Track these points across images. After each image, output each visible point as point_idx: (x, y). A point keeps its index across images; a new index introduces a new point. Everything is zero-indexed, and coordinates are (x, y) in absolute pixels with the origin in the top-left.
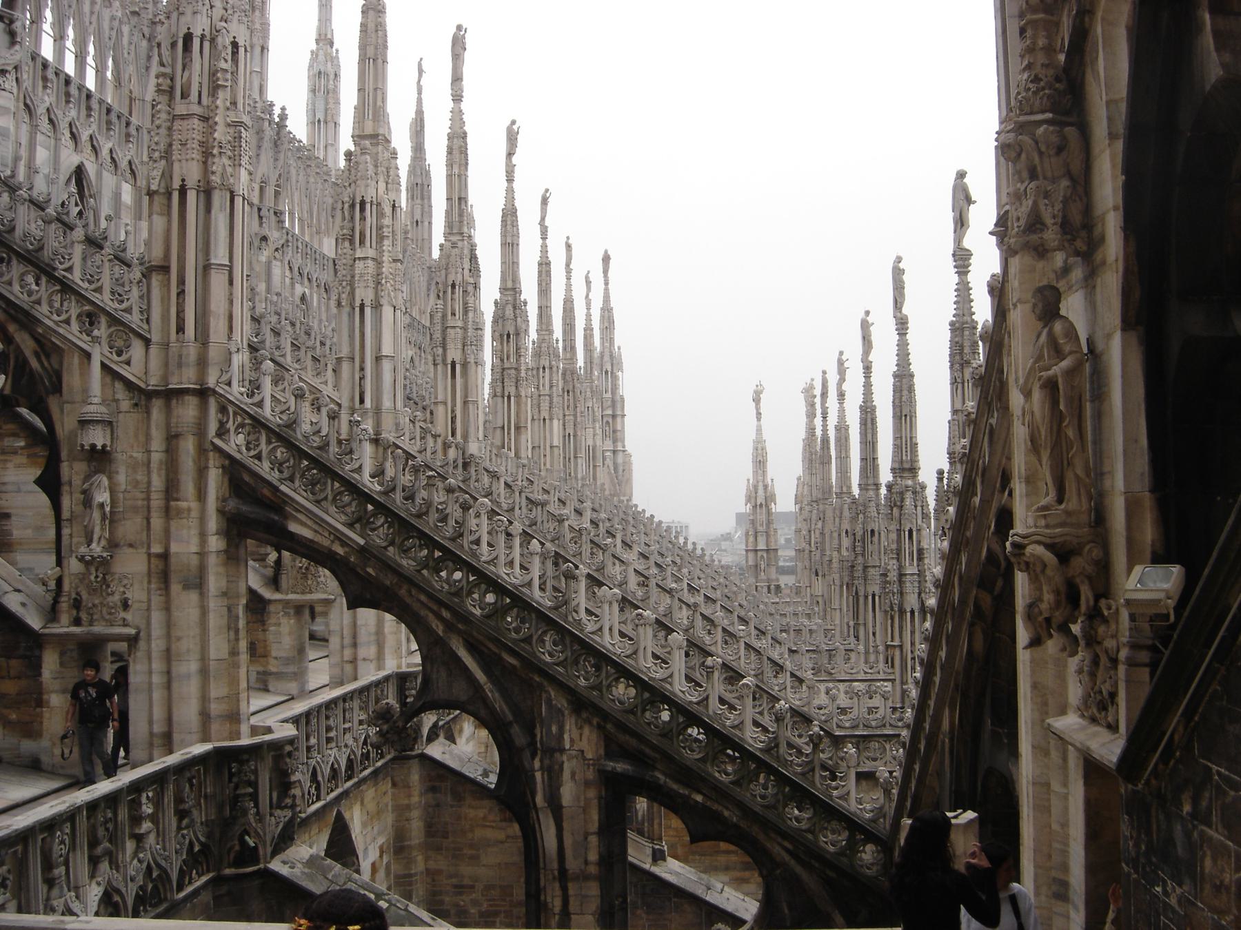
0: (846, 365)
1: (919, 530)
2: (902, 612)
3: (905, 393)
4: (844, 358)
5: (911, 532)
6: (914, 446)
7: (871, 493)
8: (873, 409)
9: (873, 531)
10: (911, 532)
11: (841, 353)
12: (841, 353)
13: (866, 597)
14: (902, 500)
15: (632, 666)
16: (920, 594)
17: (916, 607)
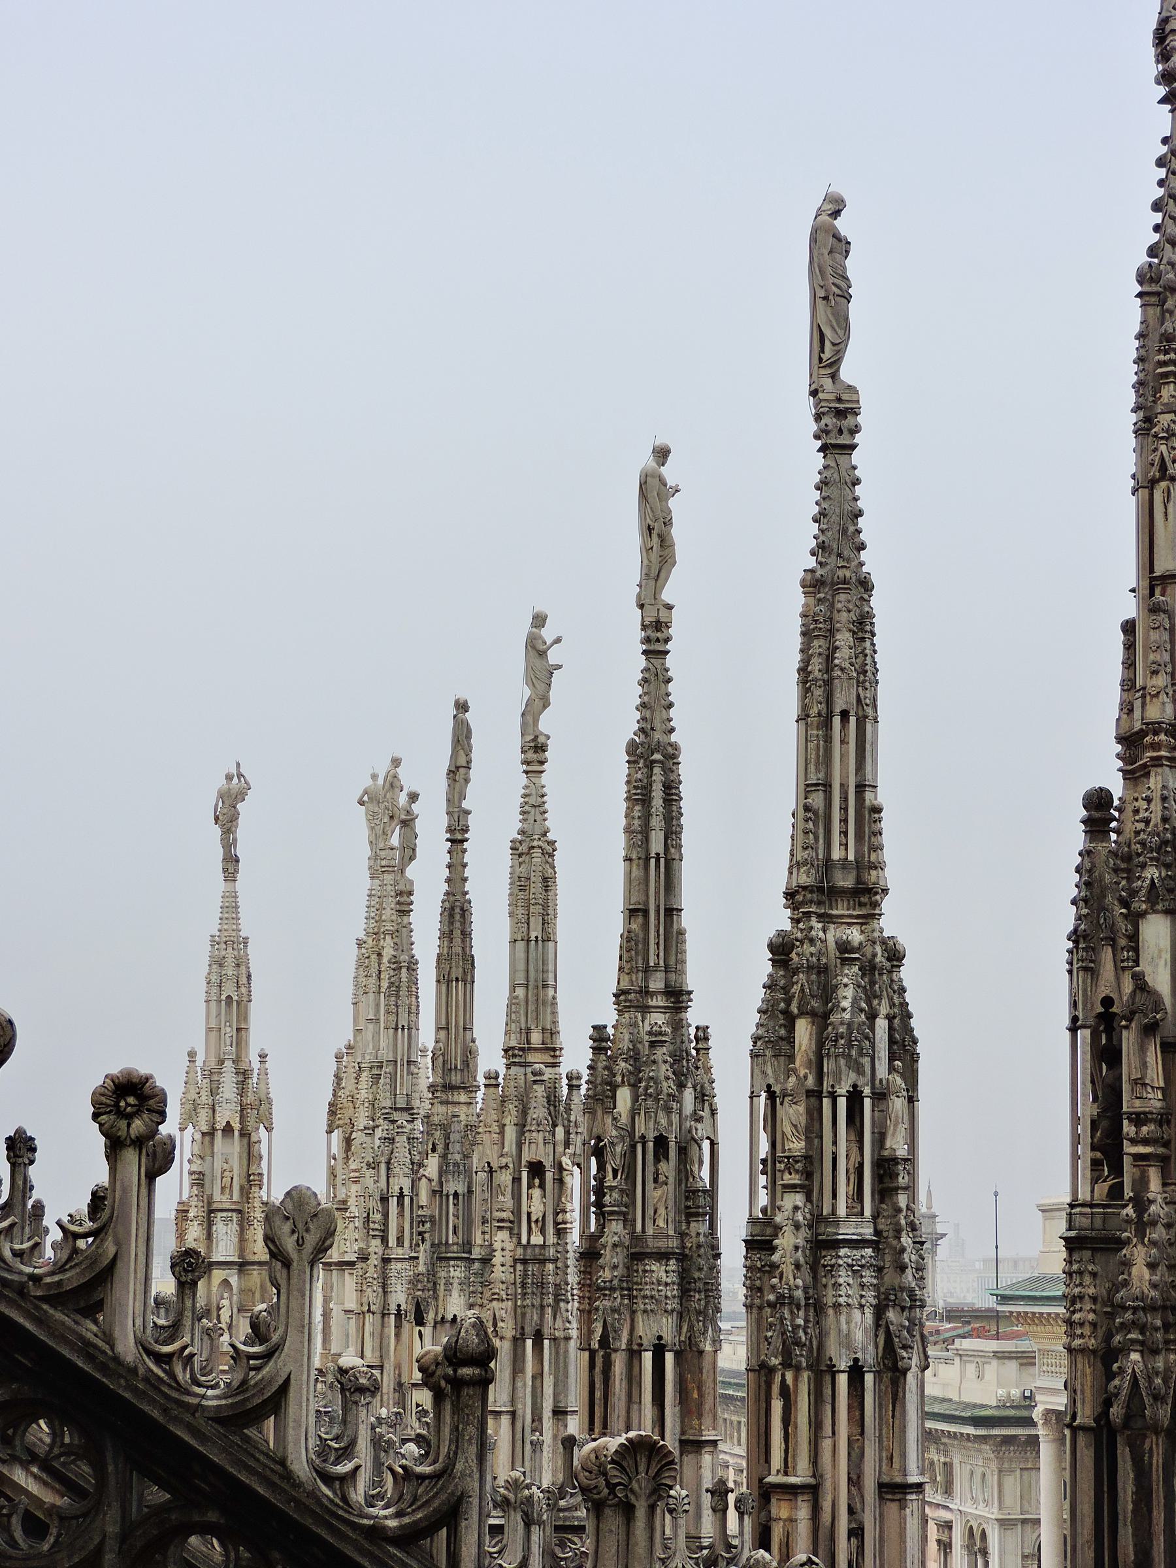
0: (553, 657)
1: (881, 1096)
2: (823, 1371)
3: (844, 638)
4: (548, 633)
5: (855, 1097)
6: (868, 817)
7: (659, 1019)
8: (671, 756)
9: (661, 1142)
10: (855, 1097)
11: (539, 620)
12: (539, 620)
13: (634, 1354)
14: (828, 993)
15: (87, 1349)
17: (868, 1357)
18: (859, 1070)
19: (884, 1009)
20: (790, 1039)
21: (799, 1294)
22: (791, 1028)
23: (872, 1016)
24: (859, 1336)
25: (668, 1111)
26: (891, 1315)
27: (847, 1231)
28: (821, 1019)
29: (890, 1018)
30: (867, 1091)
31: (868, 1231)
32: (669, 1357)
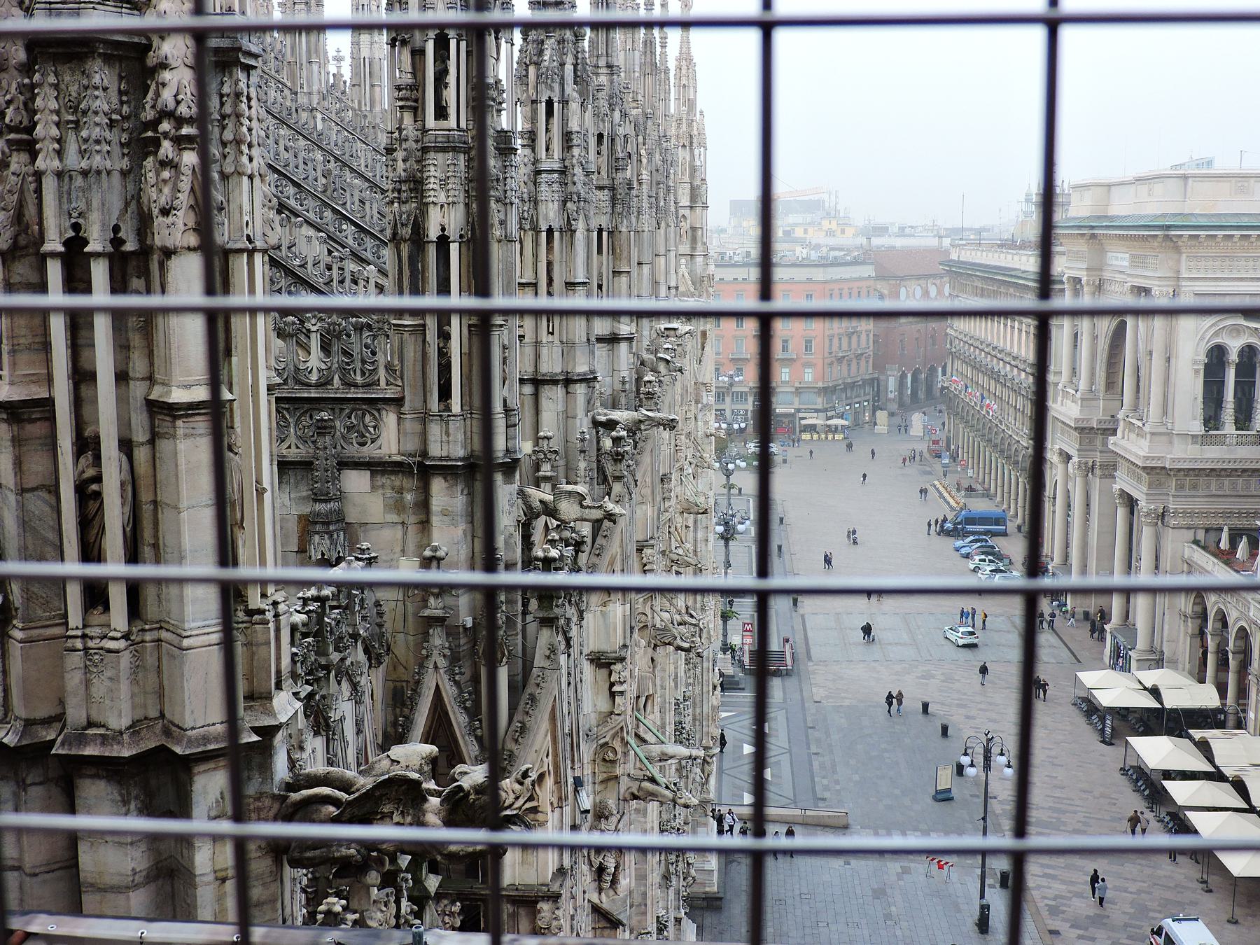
2: (536, 230)
5: (550, 103)
16: (565, 203)
18: (552, 89)
19: (569, 60)
20: (527, 76)
21: (525, 196)
22: (527, 70)
23: (562, 64)
24: (552, 215)
25: (604, 121)
26: (569, 205)
27: (544, 166)
28: (537, 64)
29: (575, 66)
30: (556, 99)
31: (556, 166)
32: (605, 234)
